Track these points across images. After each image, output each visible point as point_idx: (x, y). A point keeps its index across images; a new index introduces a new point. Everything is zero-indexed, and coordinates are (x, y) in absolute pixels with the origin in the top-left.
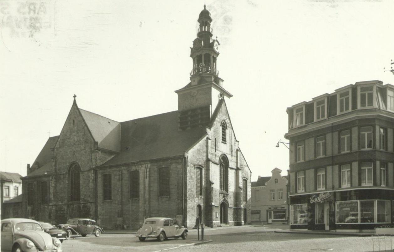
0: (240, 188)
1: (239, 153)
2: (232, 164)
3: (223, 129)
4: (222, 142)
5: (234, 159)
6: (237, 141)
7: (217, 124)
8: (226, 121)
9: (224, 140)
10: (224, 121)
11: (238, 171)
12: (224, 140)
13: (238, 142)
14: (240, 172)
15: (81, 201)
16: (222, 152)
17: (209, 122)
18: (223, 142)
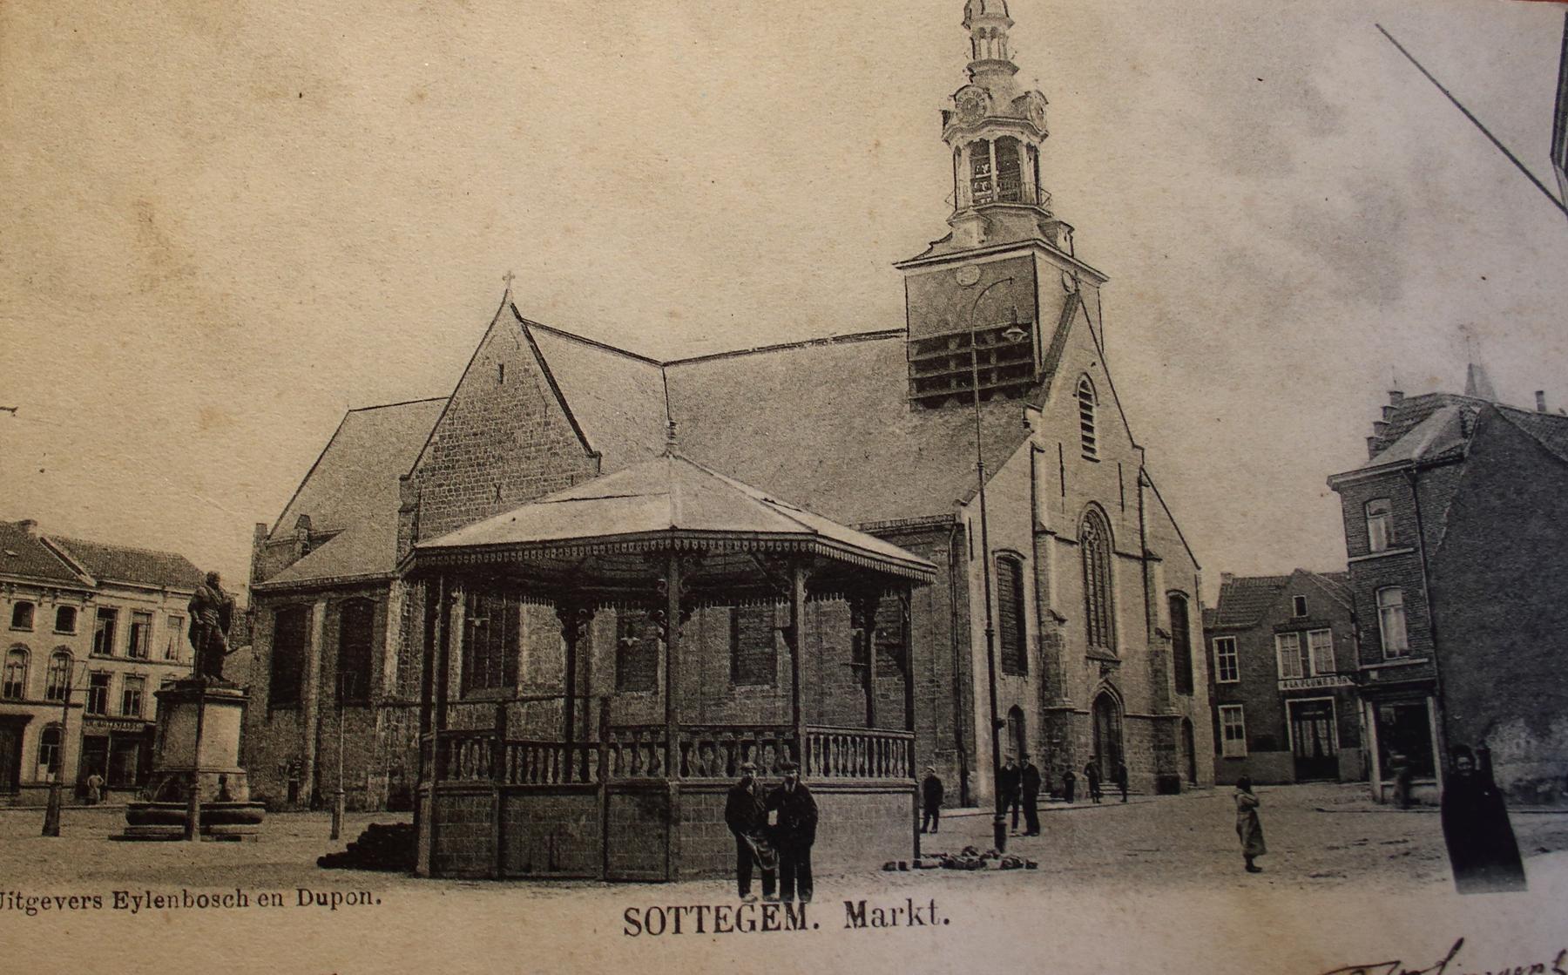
3: (1082, 405)
14: (1157, 569)
18: (1089, 454)
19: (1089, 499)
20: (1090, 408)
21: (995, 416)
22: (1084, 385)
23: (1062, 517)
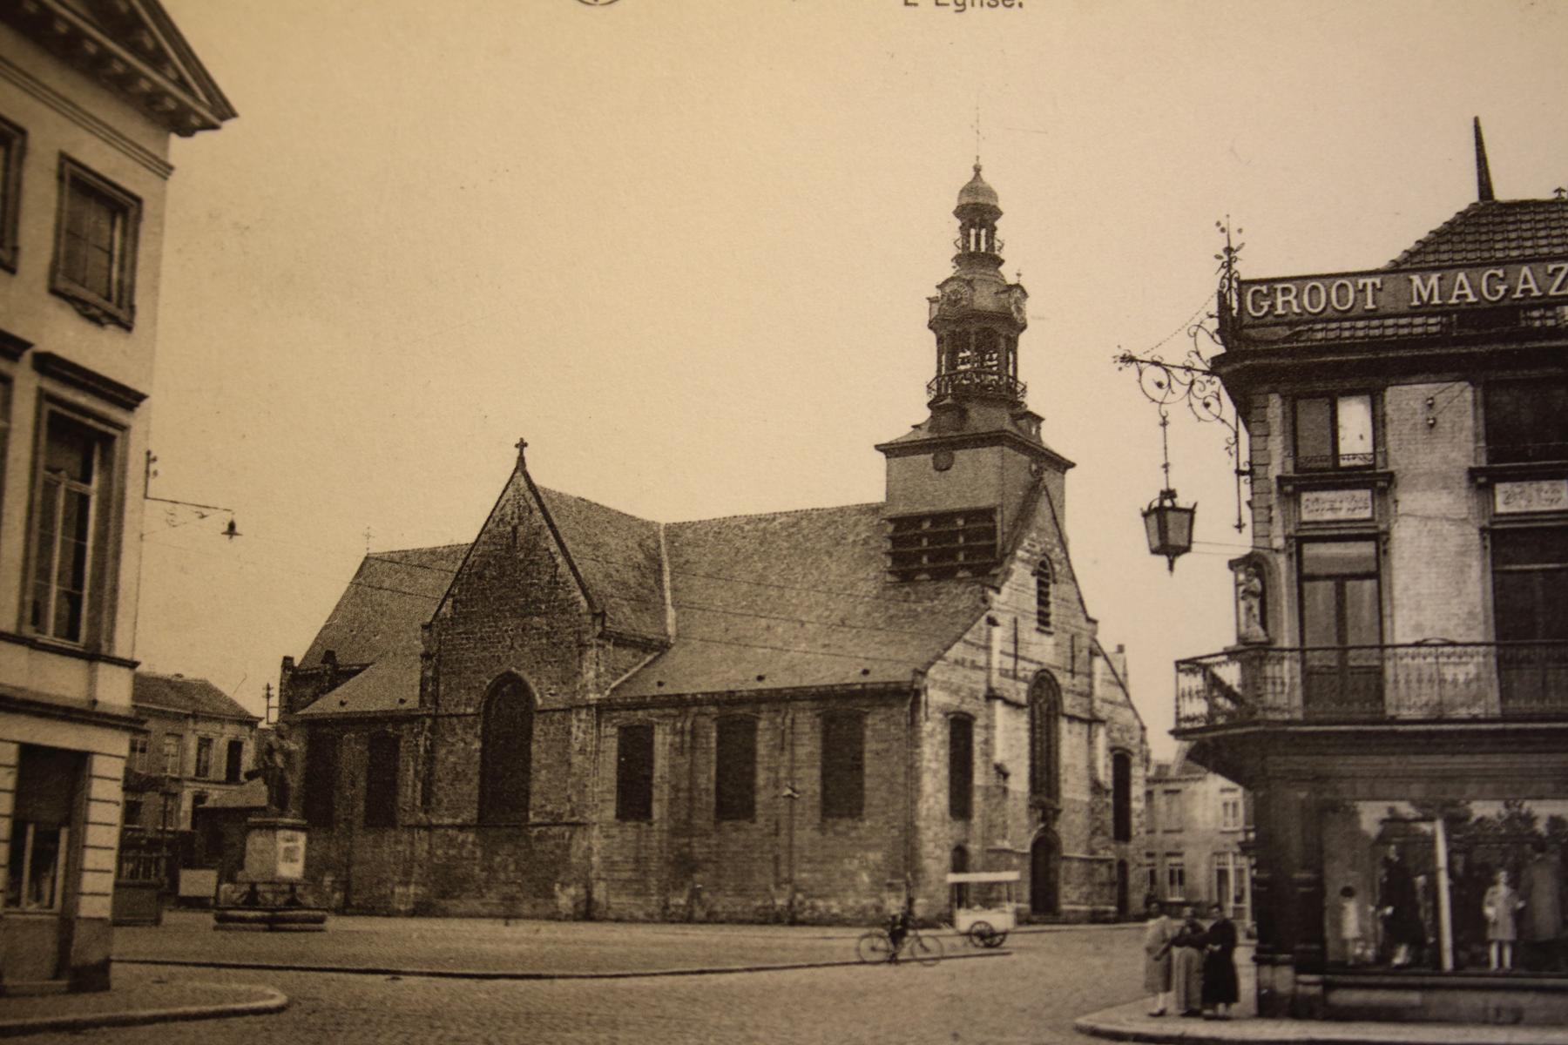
2: (1068, 703)
3: (1040, 583)
4: (1038, 630)
6: (1089, 620)
7: (1021, 576)
8: (1052, 556)
12: (1043, 619)
13: (1095, 622)
15: (531, 814)
16: (1039, 663)
20: (1047, 585)
21: (960, 596)
22: (1042, 564)
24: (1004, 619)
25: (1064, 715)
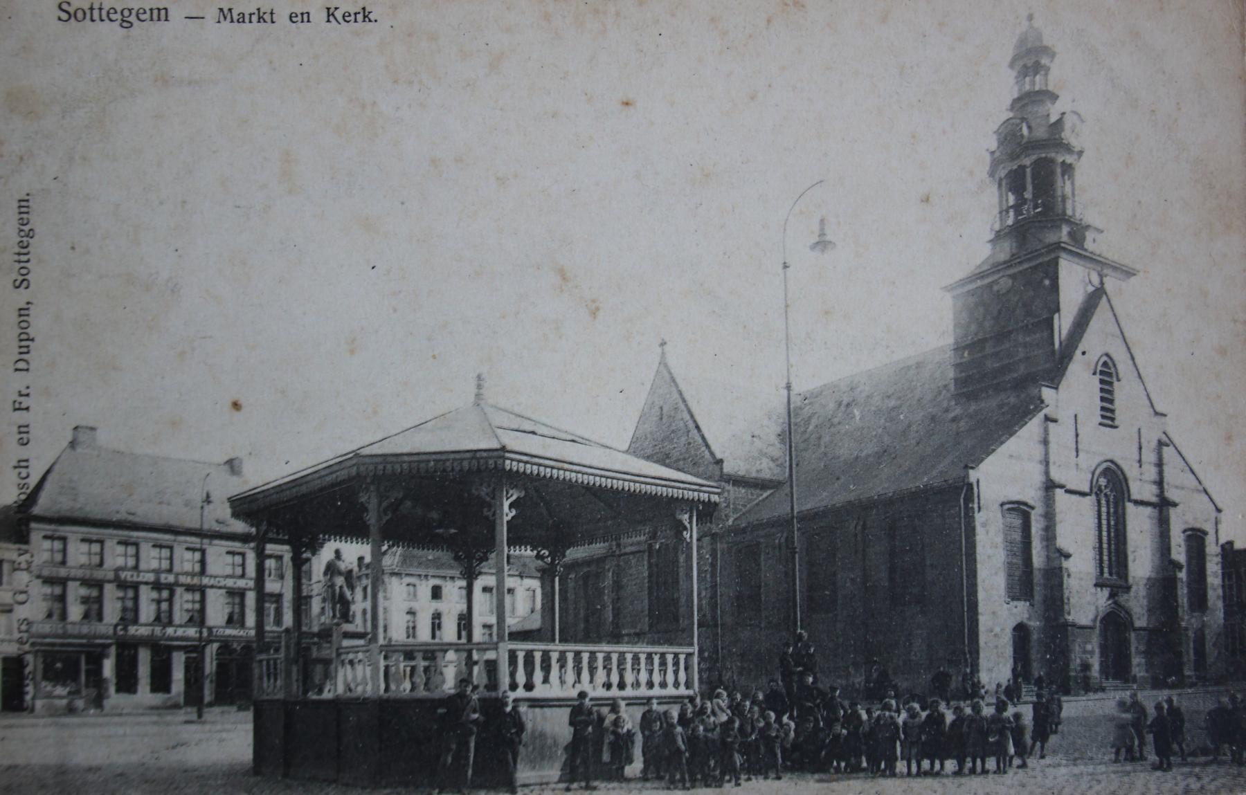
0: (1178, 566)
1: (1168, 452)
3: (1102, 381)
5: (1151, 472)
6: (1156, 413)
8: (1114, 356)
9: (1108, 417)
10: (1107, 355)
11: (1165, 513)
12: (1108, 417)
17: (1055, 370)
19: (1102, 459)
20: (1111, 384)
22: (1105, 364)
23: (1075, 472)
24: (1065, 416)
25: (1130, 500)
